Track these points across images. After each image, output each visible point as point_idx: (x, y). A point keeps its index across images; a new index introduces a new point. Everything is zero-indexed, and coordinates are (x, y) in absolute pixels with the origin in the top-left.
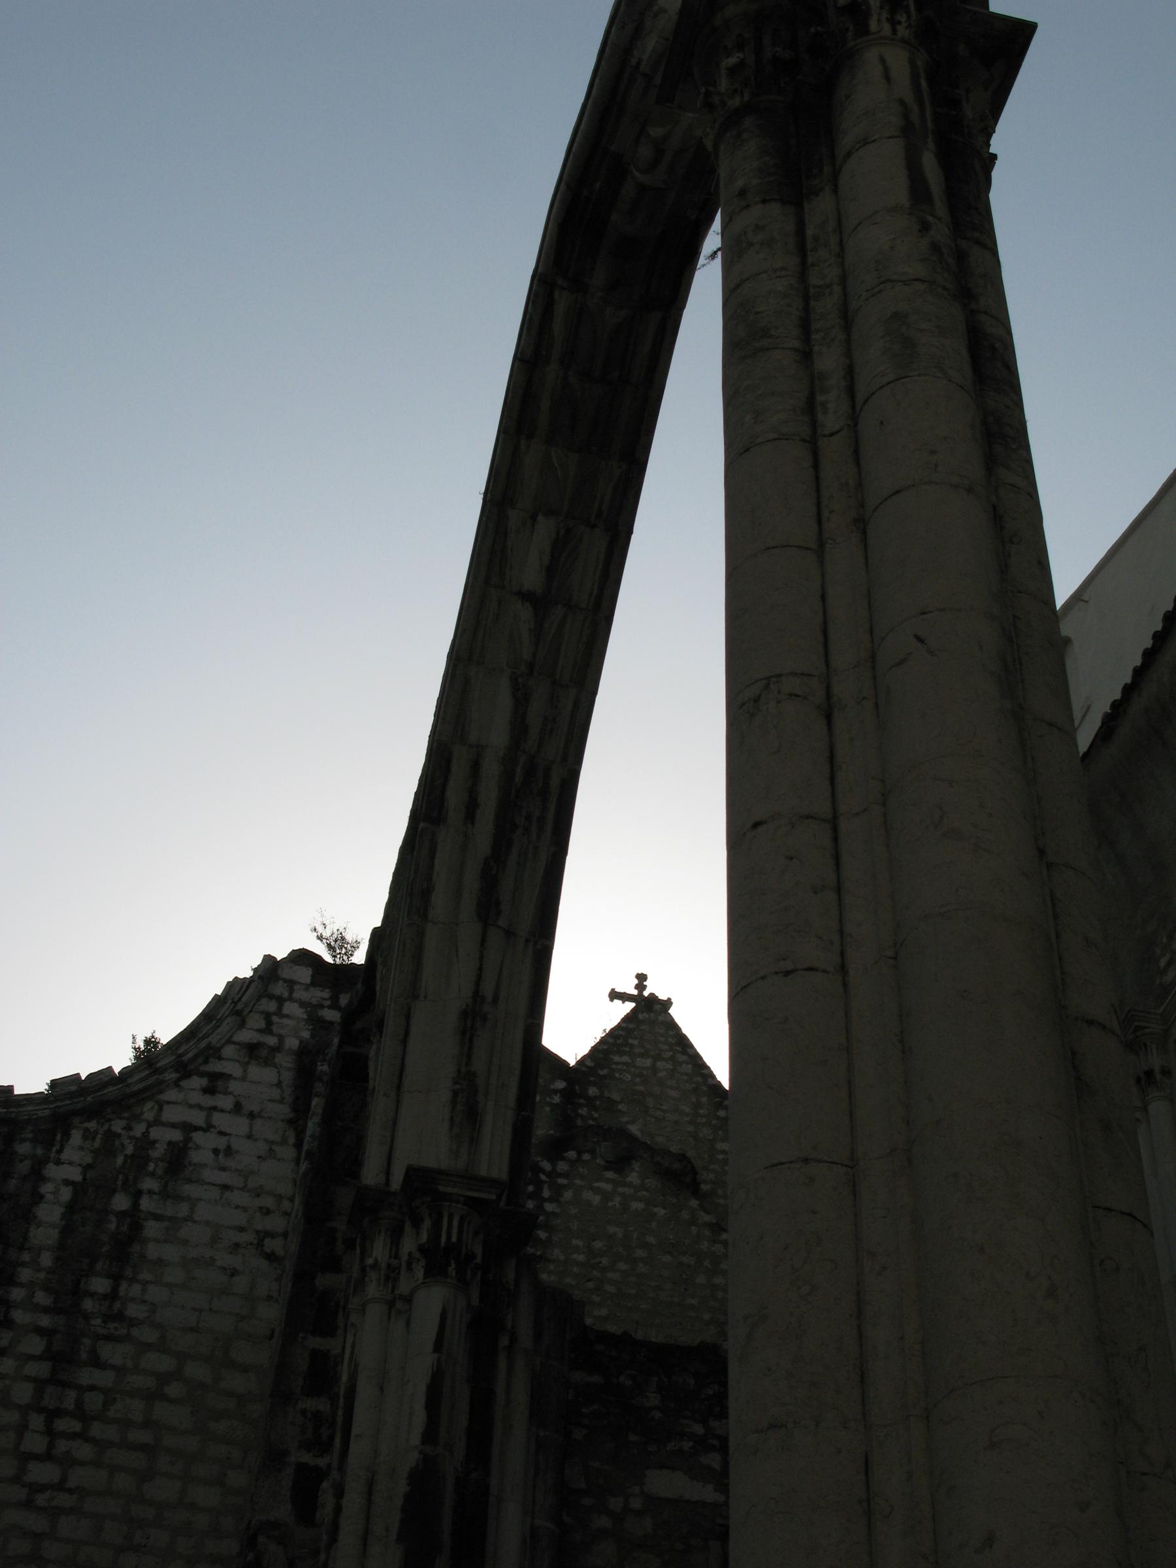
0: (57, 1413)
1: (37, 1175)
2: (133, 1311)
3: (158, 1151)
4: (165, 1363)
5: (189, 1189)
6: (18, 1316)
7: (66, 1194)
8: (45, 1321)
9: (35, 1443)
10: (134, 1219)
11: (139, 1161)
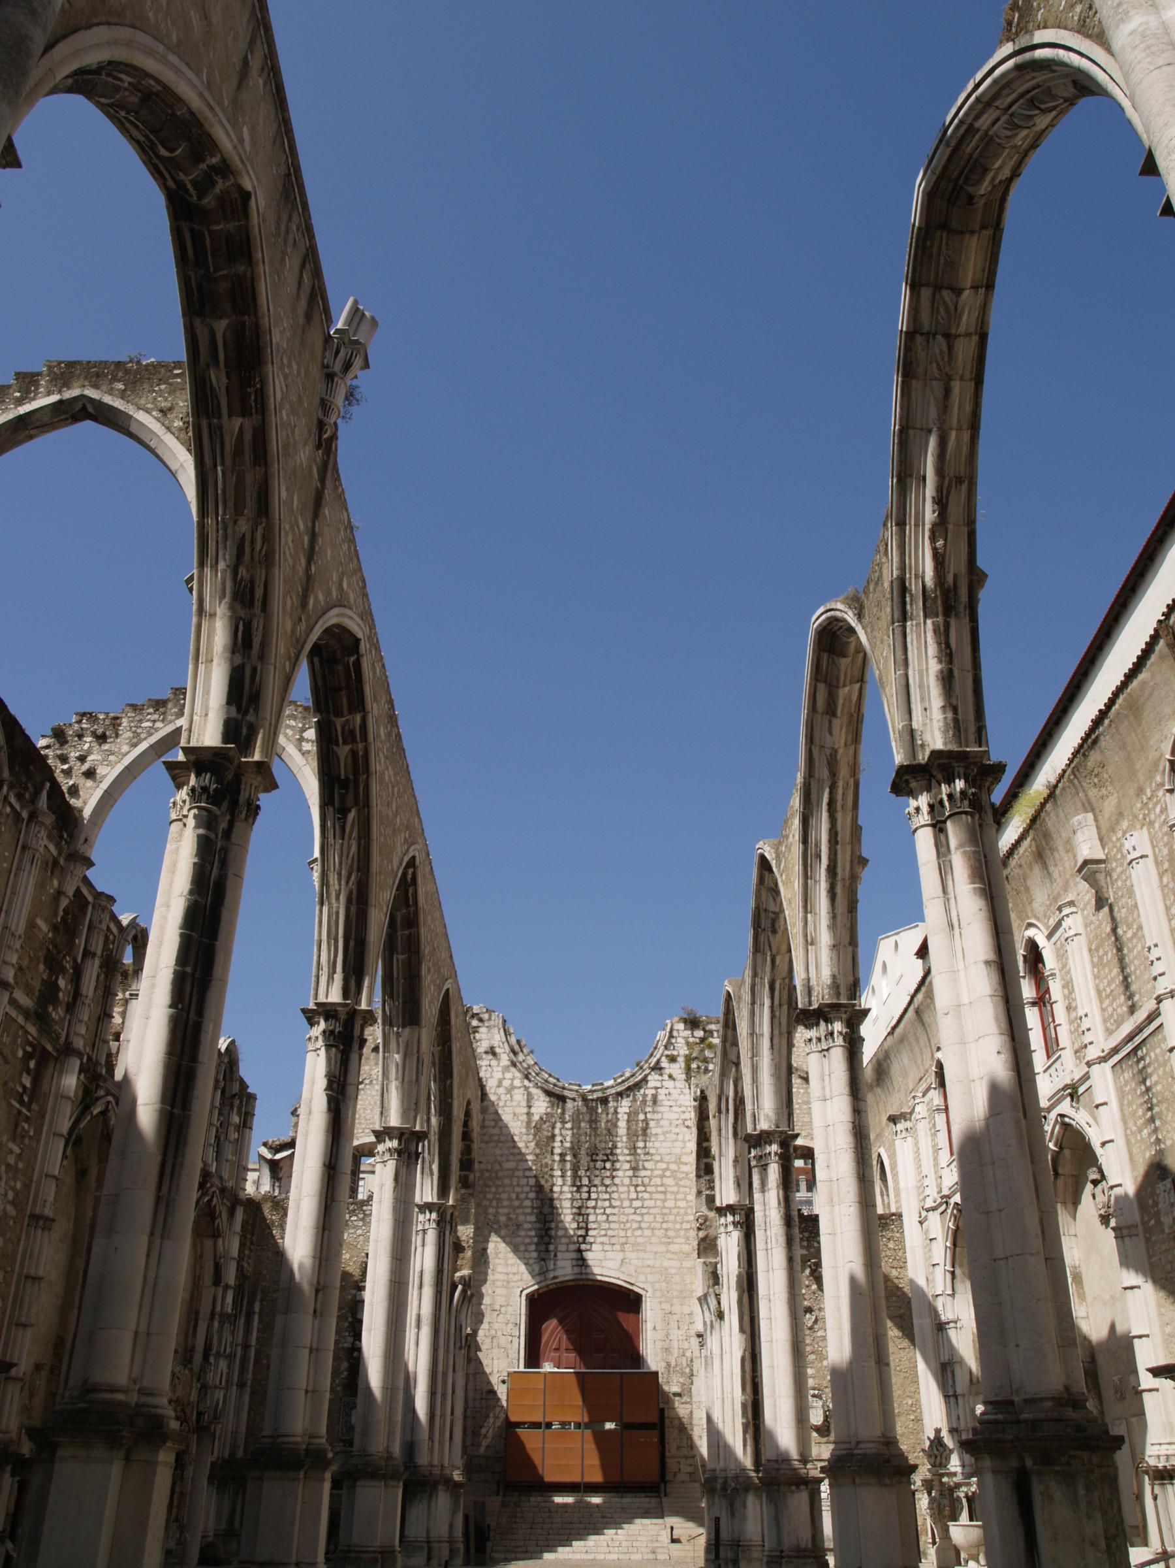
0: (637, 1186)
1: (616, 1112)
2: (652, 1151)
3: (649, 1098)
4: (664, 1166)
5: (660, 1109)
6: (620, 1158)
7: (626, 1117)
8: (628, 1158)
9: (633, 1195)
10: (646, 1120)
11: (644, 1102)
